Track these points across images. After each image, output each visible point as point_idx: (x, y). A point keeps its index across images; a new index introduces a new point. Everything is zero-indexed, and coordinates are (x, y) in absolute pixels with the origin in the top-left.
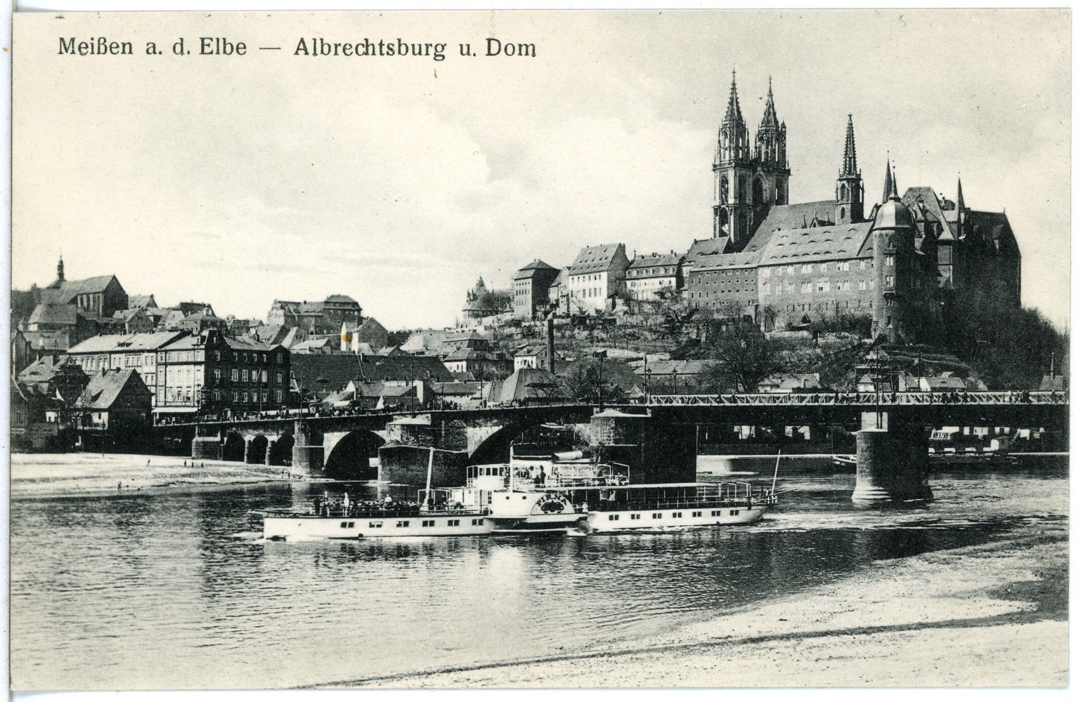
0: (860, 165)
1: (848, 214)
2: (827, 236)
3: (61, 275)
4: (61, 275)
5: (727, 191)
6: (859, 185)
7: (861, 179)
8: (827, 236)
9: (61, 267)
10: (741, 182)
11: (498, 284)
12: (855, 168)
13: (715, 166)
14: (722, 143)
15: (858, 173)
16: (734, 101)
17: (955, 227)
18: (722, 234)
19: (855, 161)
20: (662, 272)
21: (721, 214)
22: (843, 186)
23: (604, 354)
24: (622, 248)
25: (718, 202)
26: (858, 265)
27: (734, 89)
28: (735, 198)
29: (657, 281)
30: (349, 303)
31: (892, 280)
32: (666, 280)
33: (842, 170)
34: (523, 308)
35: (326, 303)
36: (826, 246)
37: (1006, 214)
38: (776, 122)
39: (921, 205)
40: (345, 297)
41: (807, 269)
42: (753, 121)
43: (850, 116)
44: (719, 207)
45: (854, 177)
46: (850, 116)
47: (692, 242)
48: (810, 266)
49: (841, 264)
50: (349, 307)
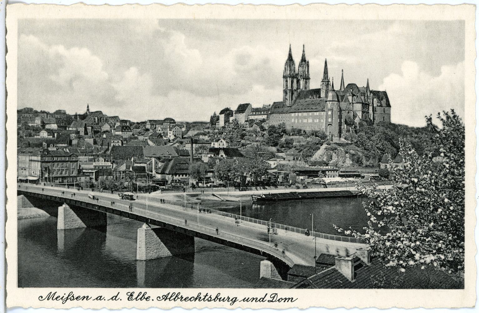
3: (88, 110)
4: (88, 110)
6: (328, 84)
7: (329, 81)
10: (292, 82)
11: (218, 114)
12: (327, 77)
13: (284, 76)
14: (286, 68)
17: (363, 98)
18: (285, 99)
19: (327, 76)
20: (263, 113)
21: (285, 92)
22: (323, 84)
23: (240, 141)
25: (284, 89)
26: (321, 113)
29: (261, 116)
32: (264, 116)
33: (323, 78)
34: (221, 123)
38: (305, 61)
39: (351, 90)
41: (305, 114)
42: (297, 60)
45: (327, 80)
47: (272, 104)
48: (306, 113)
49: (315, 113)
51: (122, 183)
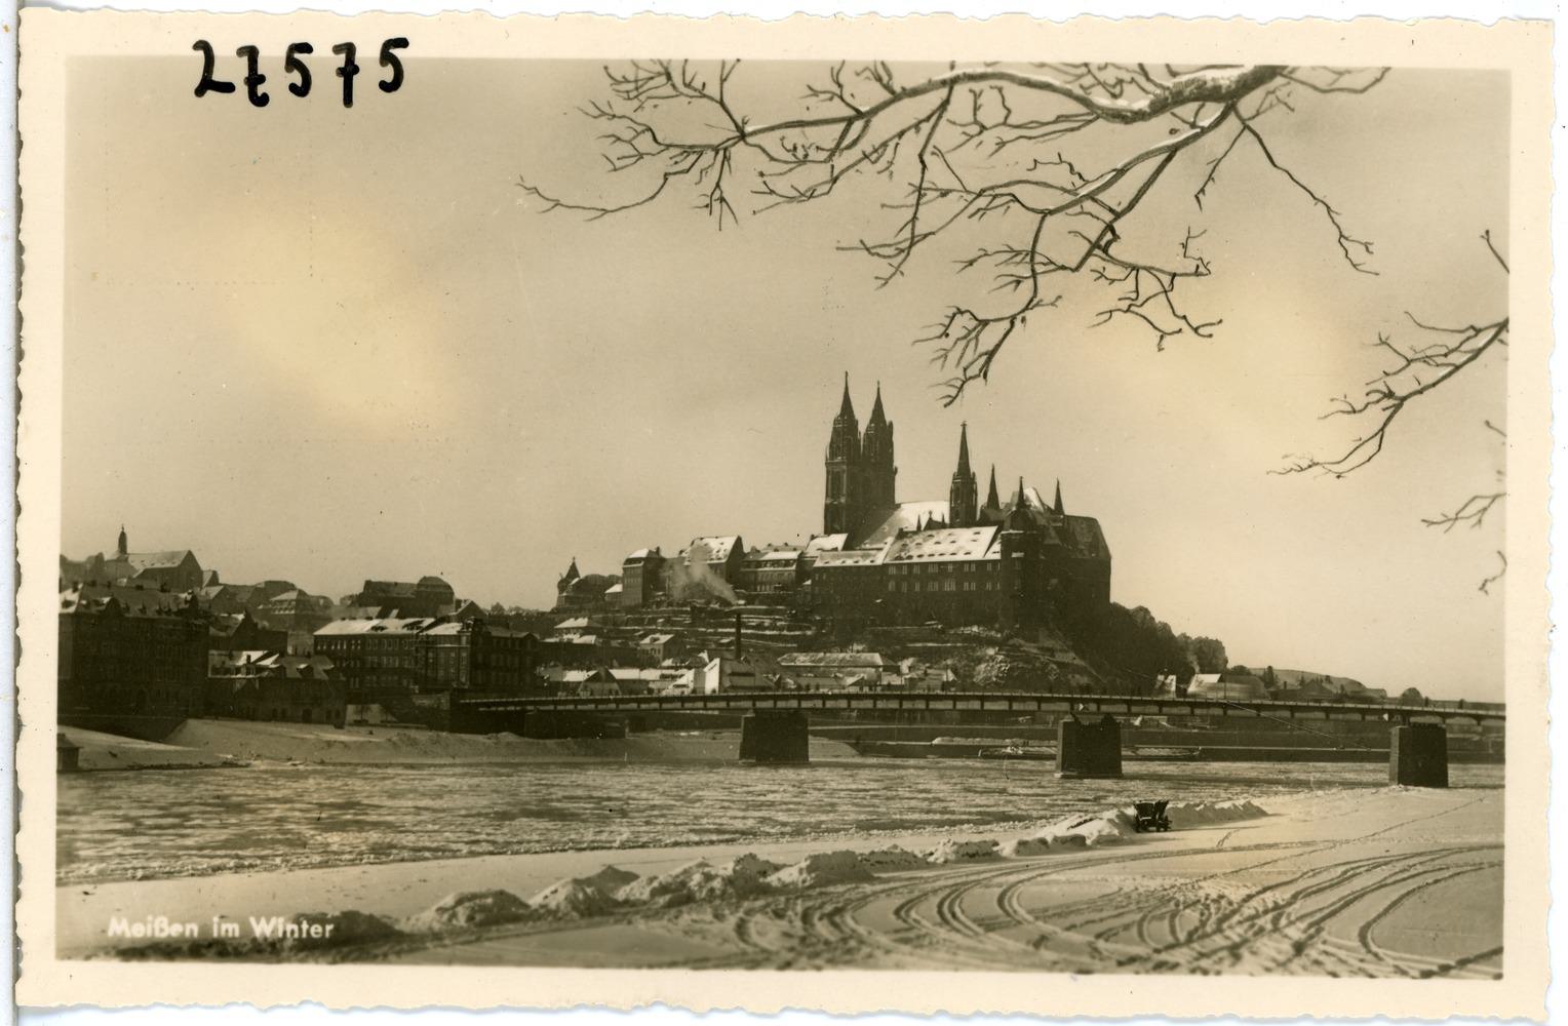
9: (123, 538)
22: (958, 489)
35: (419, 585)
36: (952, 548)
44: (832, 503)
50: (441, 590)
51: (686, 933)
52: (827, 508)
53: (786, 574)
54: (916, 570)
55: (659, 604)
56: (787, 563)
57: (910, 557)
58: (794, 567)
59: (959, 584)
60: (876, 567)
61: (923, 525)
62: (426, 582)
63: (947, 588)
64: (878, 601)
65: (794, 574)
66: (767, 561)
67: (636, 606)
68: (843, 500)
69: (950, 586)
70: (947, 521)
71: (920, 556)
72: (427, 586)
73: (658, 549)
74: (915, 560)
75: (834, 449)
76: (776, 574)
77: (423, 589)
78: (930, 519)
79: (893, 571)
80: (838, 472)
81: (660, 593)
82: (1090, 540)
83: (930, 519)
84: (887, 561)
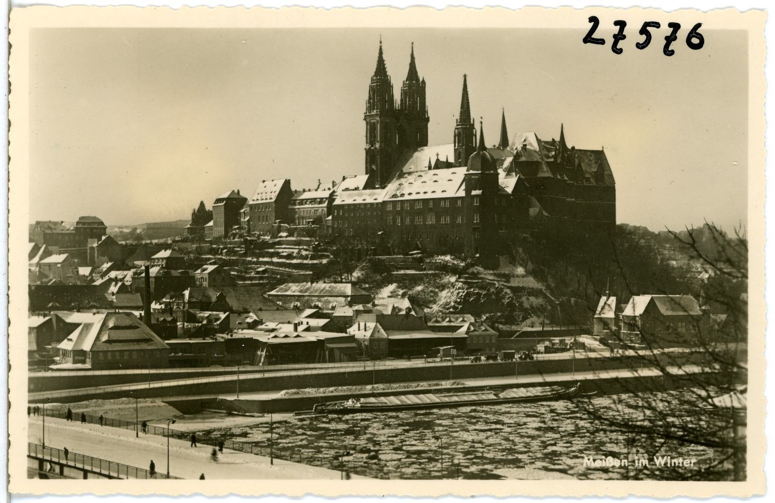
0: (474, 114)
1: (463, 156)
2: (435, 178)
5: (375, 136)
8: (435, 178)
15: (472, 122)
16: (381, 62)
22: (459, 133)
24: (287, 183)
27: (381, 53)
28: (381, 142)
30: (95, 223)
31: (476, 219)
33: (459, 121)
37: (605, 151)
38: (418, 79)
40: (95, 218)
43: (465, 76)
44: (370, 148)
46: (465, 76)
52: (368, 152)
53: (320, 210)
54: (406, 205)
55: (234, 235)
56: (321, 201)
57: (403, 195)
58: (325, 205)
59: (438, 218)
60: (377, 204)
61: (433, 164)
62: (83, 221)
63: (429, 222)
64: (380, 233)
65: (325, 209)
66: (307, 200)
67: (220, 238)
68: (378, 145)
69: (431, 220)
70: (452, 160)
71: (410, 194)
72: (84, 224)
73: (238, 191)
74: (407, 197)
75: (371, 106)
76: (313, 210)
77: (80, 226)
78: (438, 160)
79: (390, 208)
80: (374, 123)
81: (236, 227)
82: (596, 170)
83: (438, 160)
84: (386, 199)
